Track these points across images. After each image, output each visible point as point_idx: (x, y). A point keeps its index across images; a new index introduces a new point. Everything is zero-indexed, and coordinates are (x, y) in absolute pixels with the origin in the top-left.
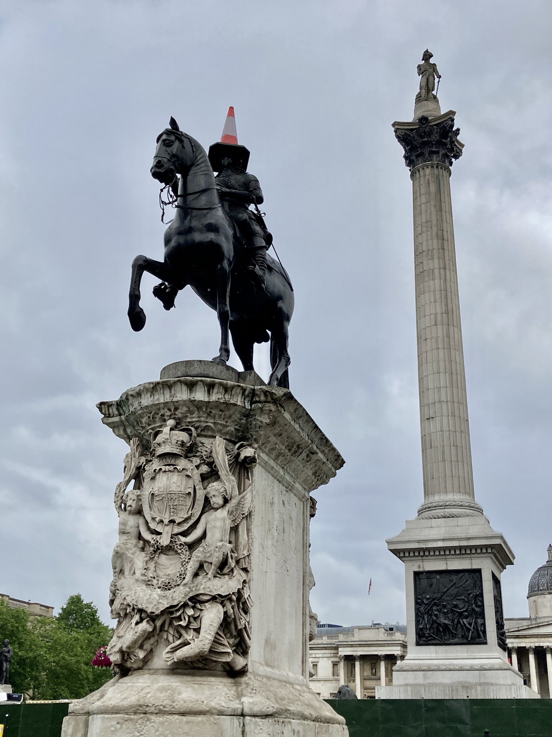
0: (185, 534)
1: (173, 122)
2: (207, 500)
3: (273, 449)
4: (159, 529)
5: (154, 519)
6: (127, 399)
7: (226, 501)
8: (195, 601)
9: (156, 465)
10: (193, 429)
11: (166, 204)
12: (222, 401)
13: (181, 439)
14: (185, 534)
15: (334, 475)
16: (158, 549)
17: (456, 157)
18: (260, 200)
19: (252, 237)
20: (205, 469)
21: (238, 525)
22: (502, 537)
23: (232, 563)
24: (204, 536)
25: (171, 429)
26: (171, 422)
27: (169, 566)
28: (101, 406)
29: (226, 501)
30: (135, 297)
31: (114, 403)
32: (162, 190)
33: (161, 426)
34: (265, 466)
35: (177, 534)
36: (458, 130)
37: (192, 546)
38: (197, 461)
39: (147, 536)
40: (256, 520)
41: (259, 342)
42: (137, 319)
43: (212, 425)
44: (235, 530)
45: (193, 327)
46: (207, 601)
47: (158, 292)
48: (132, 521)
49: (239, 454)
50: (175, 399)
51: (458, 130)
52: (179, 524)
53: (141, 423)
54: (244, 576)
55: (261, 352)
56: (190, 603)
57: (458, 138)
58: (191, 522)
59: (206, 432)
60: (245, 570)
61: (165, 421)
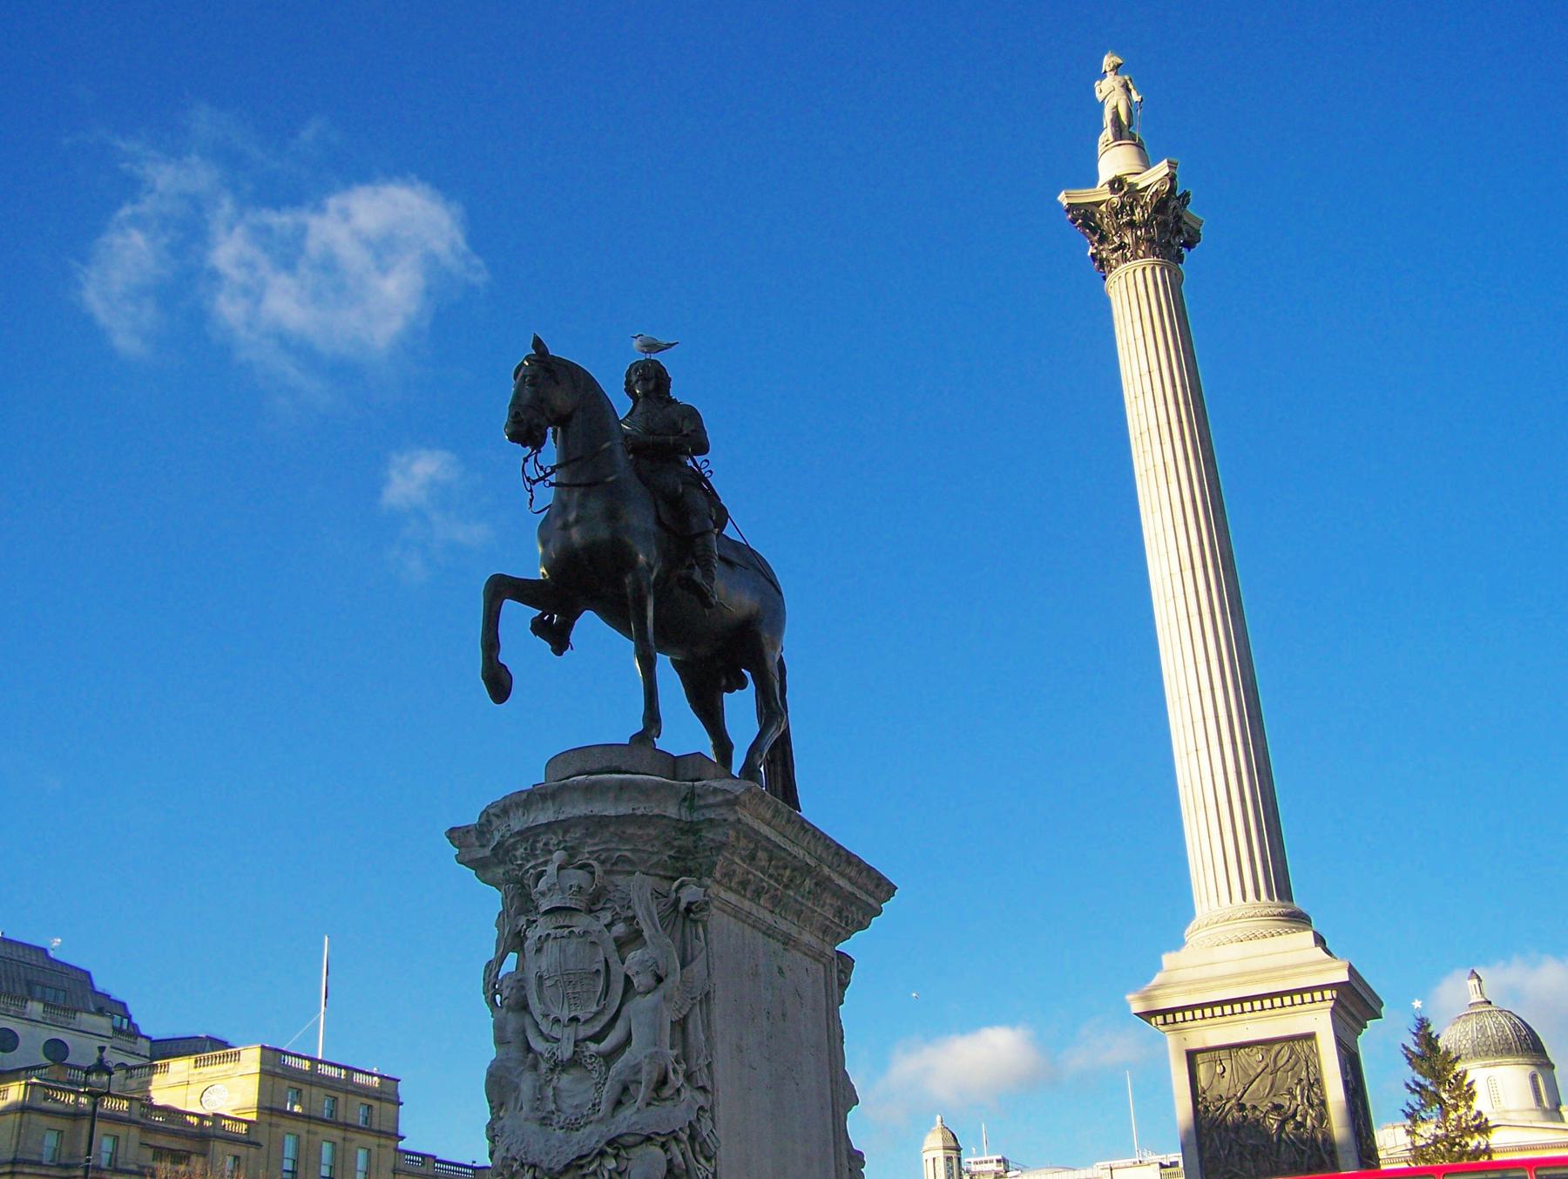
0: (597, 1038)
1: (538, 343)
2: (628, 979)
3: (744, 884)
4: (556, 1032)
5: (546, 1016)
6: (489, 821)
7: (660, 980)
8: (616, 1144)
9: (544, 926)
10: (595, 863)
11: (534, 482)
12: (639, 812)
13: (575, 882)
14: (597, 1038)
15: (878, 912)
16: (556, 1065)
17: (1189, 245)
18: (703, 448)
19: (690, 517)
20: (620, 929)
21: (685, 1018)
23: (676, 1080)
24: (628, 1040)
25: (560, 868)
26: (558, 856)
27: (574, 1090)
28: (452, 834)
29: (660, 980)
30: (491, 644)
32: (526, 460)
33: (545, 863)
34: (736, 913)
35: (584, 1040)
37: (610, 1057)
38: (607, 917)
39: (538, 1045)
40: (717, 1009)
41: (731, 690)
42: (499, 684)
43: (628, 854)
44: (681, 1025)
45: (598, 685)
46: (635, 1145)
47: (539, 627)
48: (513, 1020)
49: (678, 900)
50: (562, 817)
51: (1186, 195)
52: (586, 1022)
54: (701, 1099)
55: (740, 707)
56: (609, 1150)
58: (605, 1019)
59: (615, 865)
60: (703, 1089)
61: (551, 852)
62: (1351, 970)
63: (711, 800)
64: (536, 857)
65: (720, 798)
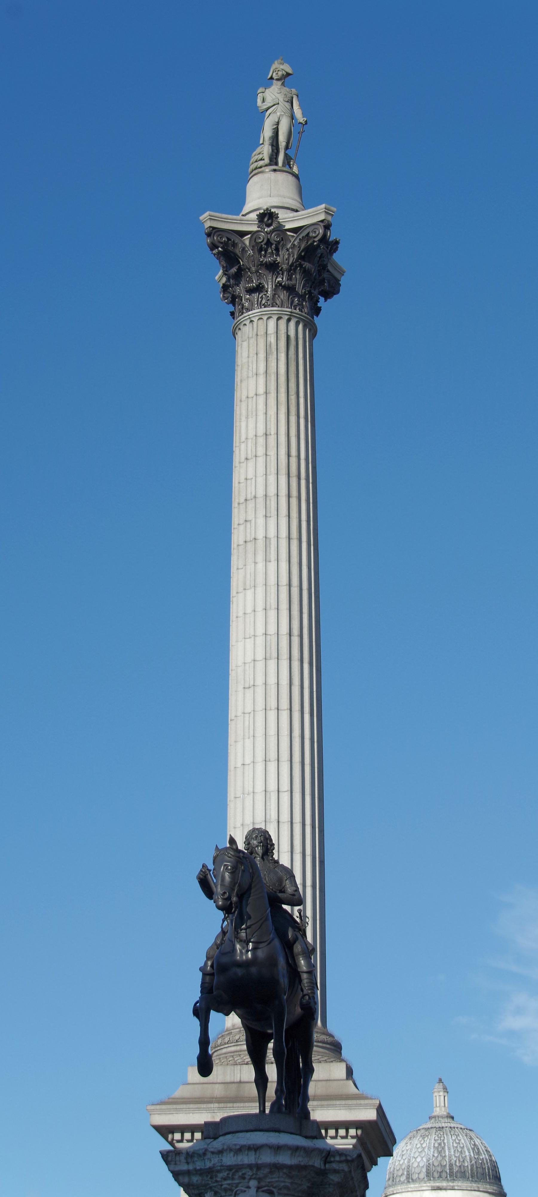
6: (204, 1154)
12: (302, 1164)
17: (327, 295)
22: (380, 1110)
31: (183, 1152)
36: (337, 243)
50: (260, 1162)
51: (337, 243)
53: (216, 1176)
57: (336, 257)
62: (380, 1110)
63: (337, 1158)
64: (233, 1179)
65: (343, 1158)
